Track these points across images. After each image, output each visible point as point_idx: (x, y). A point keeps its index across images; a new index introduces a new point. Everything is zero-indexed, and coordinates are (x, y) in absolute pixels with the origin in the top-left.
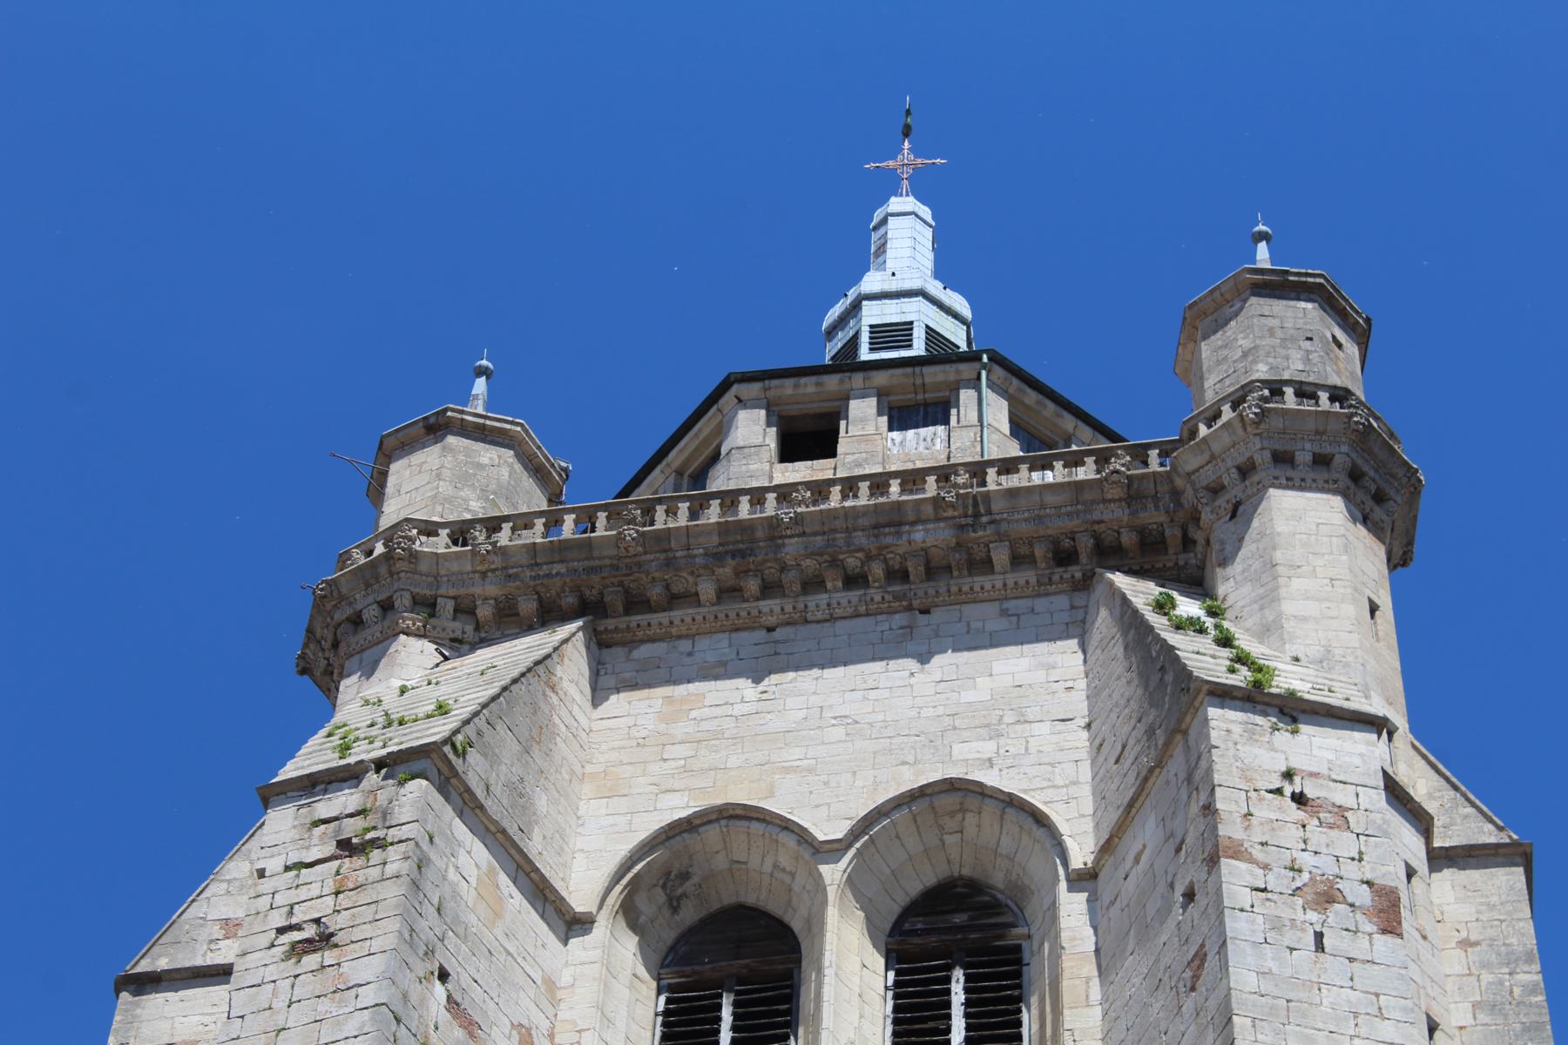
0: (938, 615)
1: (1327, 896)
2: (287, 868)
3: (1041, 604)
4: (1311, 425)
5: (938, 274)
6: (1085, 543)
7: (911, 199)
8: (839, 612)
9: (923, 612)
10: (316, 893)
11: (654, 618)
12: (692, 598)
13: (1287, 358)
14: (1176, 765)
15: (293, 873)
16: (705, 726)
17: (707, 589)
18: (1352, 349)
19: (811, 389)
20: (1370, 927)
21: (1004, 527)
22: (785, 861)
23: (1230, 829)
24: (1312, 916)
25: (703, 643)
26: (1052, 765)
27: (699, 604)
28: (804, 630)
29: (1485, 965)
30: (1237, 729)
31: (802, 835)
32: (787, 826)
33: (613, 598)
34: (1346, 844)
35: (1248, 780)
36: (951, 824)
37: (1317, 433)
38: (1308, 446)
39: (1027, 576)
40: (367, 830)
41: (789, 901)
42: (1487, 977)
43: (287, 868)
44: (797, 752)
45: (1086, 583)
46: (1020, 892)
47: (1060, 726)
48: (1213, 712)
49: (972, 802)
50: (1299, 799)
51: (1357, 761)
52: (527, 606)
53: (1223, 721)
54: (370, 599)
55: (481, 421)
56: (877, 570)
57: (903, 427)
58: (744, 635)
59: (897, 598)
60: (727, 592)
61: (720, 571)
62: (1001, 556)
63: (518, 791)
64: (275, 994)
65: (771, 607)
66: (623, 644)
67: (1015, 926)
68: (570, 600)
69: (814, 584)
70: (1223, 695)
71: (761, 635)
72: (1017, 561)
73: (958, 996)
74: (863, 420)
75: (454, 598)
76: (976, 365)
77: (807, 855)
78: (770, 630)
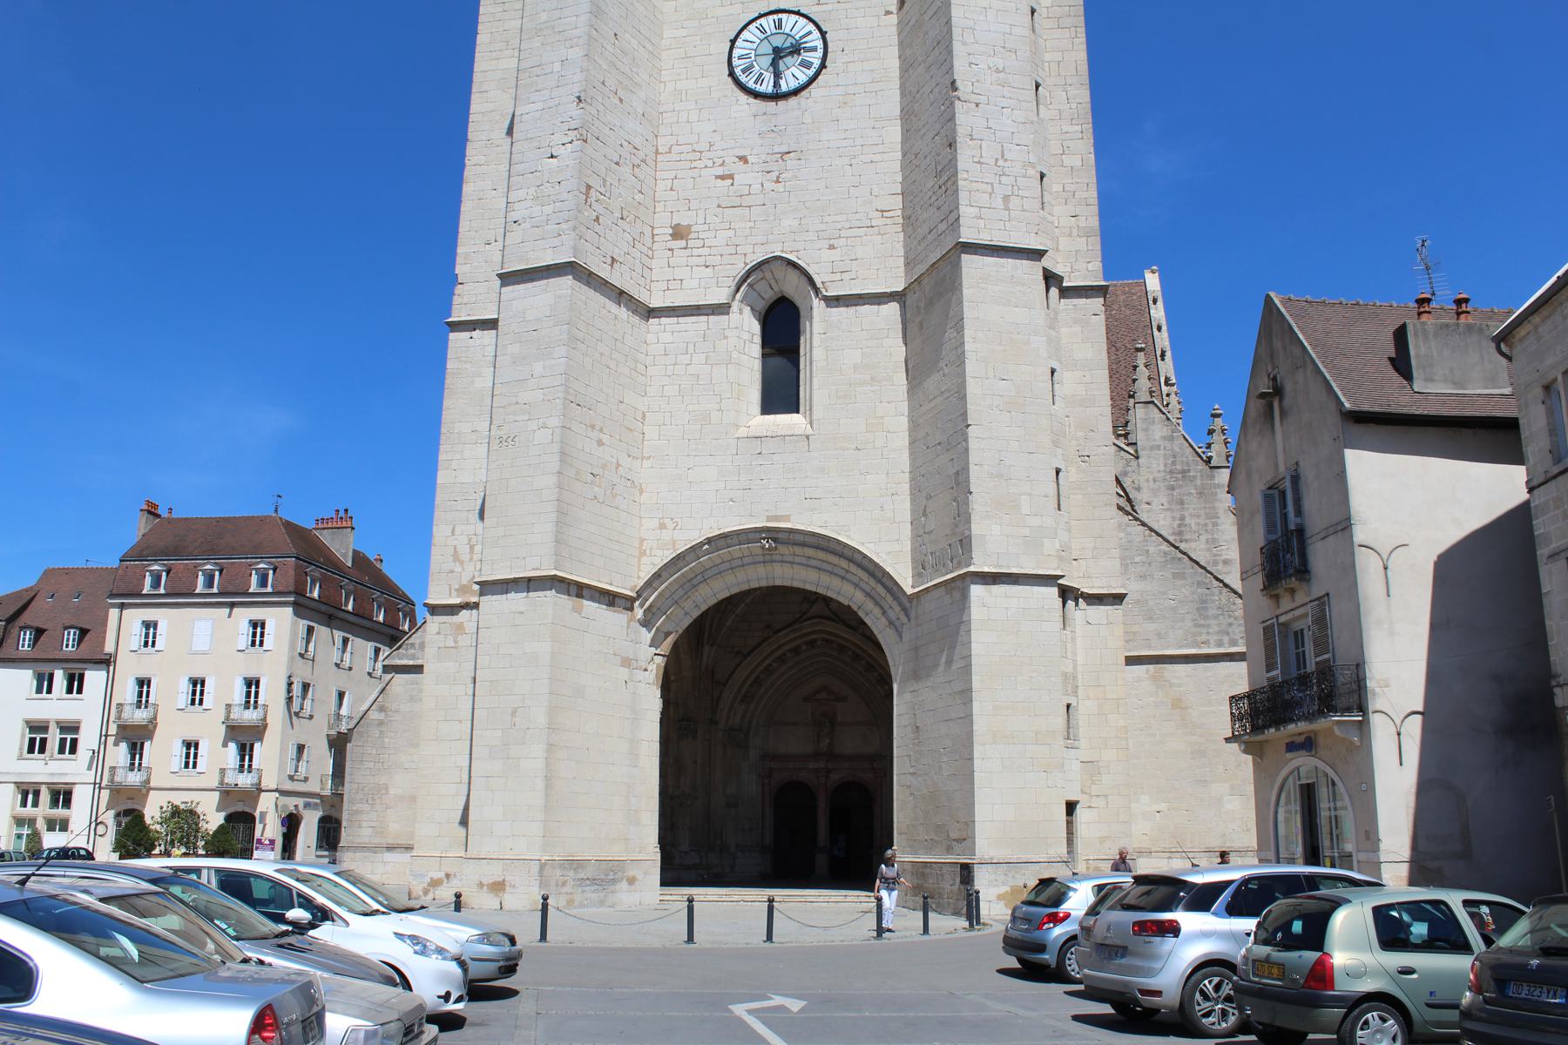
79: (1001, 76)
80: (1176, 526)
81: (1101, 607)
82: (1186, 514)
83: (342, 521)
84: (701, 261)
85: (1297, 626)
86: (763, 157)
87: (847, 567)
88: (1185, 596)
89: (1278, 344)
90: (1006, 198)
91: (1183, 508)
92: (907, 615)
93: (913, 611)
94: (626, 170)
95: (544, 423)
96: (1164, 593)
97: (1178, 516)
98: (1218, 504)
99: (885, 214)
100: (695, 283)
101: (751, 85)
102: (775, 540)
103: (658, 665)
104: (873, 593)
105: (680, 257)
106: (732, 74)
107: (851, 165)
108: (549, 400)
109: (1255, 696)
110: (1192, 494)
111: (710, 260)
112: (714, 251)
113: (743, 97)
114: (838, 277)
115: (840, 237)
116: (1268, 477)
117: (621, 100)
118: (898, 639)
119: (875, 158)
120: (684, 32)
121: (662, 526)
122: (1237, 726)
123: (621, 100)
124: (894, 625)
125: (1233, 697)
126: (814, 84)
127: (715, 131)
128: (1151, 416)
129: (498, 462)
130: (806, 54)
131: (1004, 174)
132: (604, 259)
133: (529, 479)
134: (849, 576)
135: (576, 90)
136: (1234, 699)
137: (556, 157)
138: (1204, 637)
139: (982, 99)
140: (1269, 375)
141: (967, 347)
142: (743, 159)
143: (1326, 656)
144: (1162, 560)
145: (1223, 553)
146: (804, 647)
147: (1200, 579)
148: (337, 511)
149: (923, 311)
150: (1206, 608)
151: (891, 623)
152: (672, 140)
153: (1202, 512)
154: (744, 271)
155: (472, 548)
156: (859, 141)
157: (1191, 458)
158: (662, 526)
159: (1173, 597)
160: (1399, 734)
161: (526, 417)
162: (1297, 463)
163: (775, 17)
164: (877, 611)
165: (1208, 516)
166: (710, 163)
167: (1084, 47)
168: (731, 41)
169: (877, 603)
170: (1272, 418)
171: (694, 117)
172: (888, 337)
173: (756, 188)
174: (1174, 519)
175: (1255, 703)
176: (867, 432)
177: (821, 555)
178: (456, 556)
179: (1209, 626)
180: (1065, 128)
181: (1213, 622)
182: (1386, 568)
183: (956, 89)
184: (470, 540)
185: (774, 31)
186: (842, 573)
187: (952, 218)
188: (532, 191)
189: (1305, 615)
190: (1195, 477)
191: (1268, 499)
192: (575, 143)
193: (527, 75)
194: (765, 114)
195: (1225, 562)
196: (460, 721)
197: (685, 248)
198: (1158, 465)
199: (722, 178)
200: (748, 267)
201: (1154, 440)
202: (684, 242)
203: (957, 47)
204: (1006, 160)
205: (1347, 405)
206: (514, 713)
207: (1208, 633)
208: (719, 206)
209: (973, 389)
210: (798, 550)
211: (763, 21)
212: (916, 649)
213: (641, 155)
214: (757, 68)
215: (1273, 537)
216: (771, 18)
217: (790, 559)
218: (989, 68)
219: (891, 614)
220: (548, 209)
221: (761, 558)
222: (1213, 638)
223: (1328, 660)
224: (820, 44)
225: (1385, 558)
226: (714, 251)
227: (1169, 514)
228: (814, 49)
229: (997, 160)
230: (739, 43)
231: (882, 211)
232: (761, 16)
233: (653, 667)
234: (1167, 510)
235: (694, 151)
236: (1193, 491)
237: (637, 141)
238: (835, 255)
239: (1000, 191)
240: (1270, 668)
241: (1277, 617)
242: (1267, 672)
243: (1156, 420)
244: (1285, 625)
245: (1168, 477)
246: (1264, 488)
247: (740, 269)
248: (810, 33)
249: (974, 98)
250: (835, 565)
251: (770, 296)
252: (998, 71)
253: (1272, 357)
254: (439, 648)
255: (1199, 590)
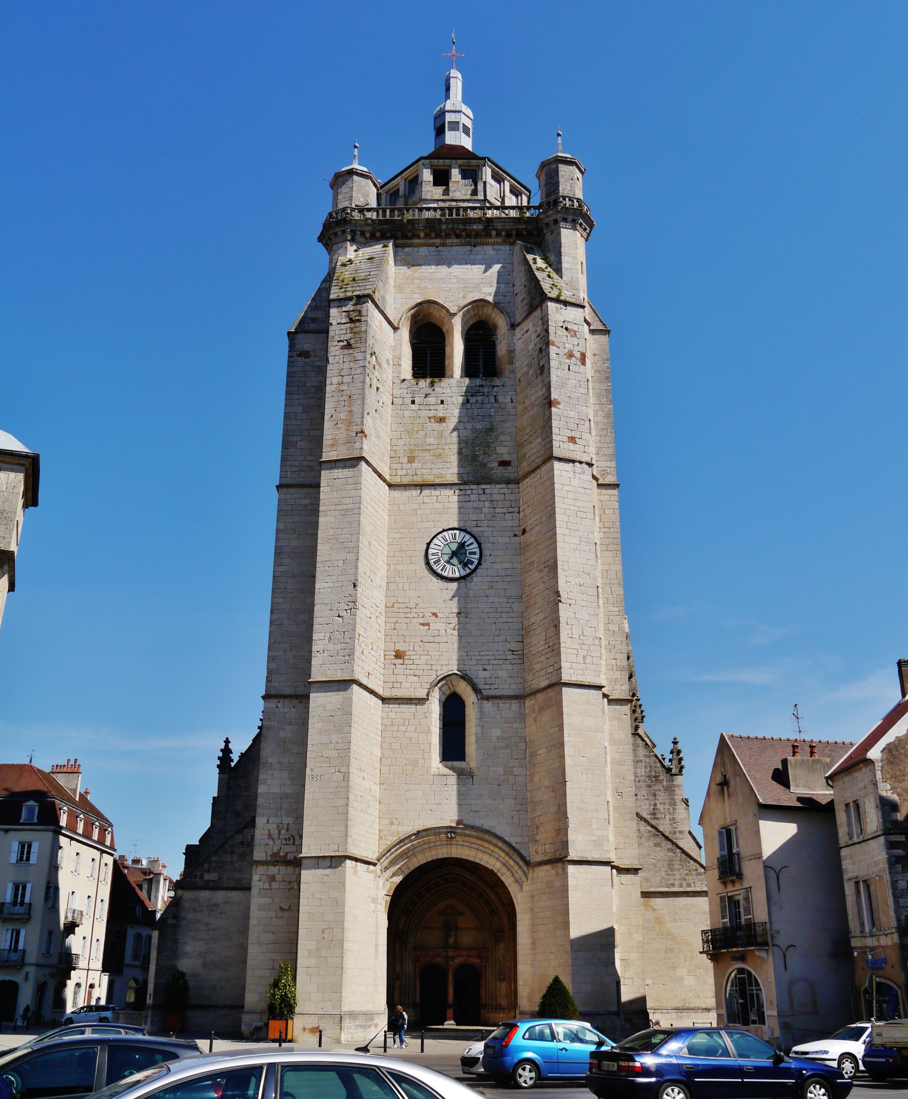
0: (478, 248)
1: (570, 355)
2: (338, 324)
3: (502, 247)
4: (573, 211)
5: (465, 101)
6: (514, 232)
7: (456, 71)
8: (454, 244)
9: (475, 246)
10: (345, 332)
11: (409, 241)
12: (419, 237)
13: (566, 185)
14: (538, 313)
15: (338, 326)
16: (423, 275)
17: (422, 234)
18: (581, 179)
19: (442, 164)
20: (579, 364)
21: (495, 227)
22: (442, 315)
23: (552, 338)
24: (568, 361)
25: (421, 249)
26: (505, 296)
27: (419, 238)
28: (445, 249)
29: (598, 361)
30: (554, 309)
31: (447, 310)
32: (444, 307)
33: (399, 234)
34: (576, 341)
35: (555, 323)
36: (480, 309)
37: (573, 213)
38: (571, 217)
39: (499, 240)
40: (356, 316)
41: (442, 325)
42: (599, 364)
43: (338, 324)
44: (445, 285)
45: (513, 244)
46: (495, 327)
47: (507, 285)
48: (549, 304)
49: (487, 304)
50: (566, 329)
51: (579, 318)
52: (378, 234)
53: (551, 305)
54: (339, 229)
55: (361, 172)
56: (464, 234)
57: (465, 179)
58: (431, 249)
59: (468, 242)
60: (427, 236)
61: (426, 231)
62: (494, 233)
63: (383, 297)
64: (339, 359)
65: (437, 241)
66: (401, 247)
67: (493, 335)
68: (389, 234)
69: (448, 236)
70: (552, 300)
71: (434, 248)
72: (498, 235)
73: (481, 353)
74: (455, 175)
75: (360, 231)
76: (484, 161)
77: (448, 316)
78: (437, 247)
79: (582, 588)
80: (651, 810)
81: (629, 876)
82: (658, 802)
83: (73, 770)
84: (412, 672)
85: (737, 898)
86: (447, 615)
87: (493, 849)
88: (661, 857)
89: (727, 761)
90: (584, 657)
91: (656, 799)
92: (526, 877)
93: (530, 875)
94: (373, 619)
95: (339, 769)
96: (649, 855)
97: (653, 803)
98: (676, 797)
99: (514, 653)
100: (409, 685)
101: (439, 571)
102: (454, 833)
103: (386, 901)
104: (507, 864)
105: (400, 669)
106: (428, 563)
107: (495, 623)
108: (341, 757)
109: (715, 932)
110: (660, 790)
111: (417, 673)
112: (419, 667)
113: (434, 579)
114: (488, 687)
115: (489, 664)
116: (721, 823)
117: (371, 580)
118: (520, 890)
119: (510, 620)
120: (400, 535)
121: (392, 823)
122: (705, 946)
123: (371, 580)
124: (518, 882)
125: (703, 931)
126: (474, 574)
127: (419, 597)
128: (638, 742)
129: (312, 789)
130: (470, 556)
131: (583, 644)
132: (365, 674)
133: (330, 800)
134: (494, 854)
135: (352, 578)
136: (704, 932)
137: (342, 617)
138: (672, 882)
139: (573, 602)
140: (722, 773)
141: (565, 739)
142: (435, 615)
143: (750, 917)
144: (648, 835)
145: (679, 826)
146: (442, 882)
147: (669, 847)
148: (69, 760)
149: (536, 712)
150: (673, 865)
151: (516, 881)
152: (394, 600)
153: (667, 801)
154: (436, 681)
155: (279, 832)
156: (499, 610)
157: (660, 769)
158: (392, 823)
159: (653, 857)
160: (784, 956)
161: (328, 765)
162: (736, 821)
163: (452, 532)
164: (508, 874)
165: (670, 804)
166: (416, 616)
167: (620, 562)
168: (427, 543)
169: (509, 869)
170: (724, 795)
171: (407, 587)
172: (515, 722)
173: (442, 632)
174: (650, 805)
175: (716, 935)
176: (504, 775)
177: (479, 842)
178: (270, 836)
179: (675, 875)
180: (611, 609)
181: (676, 873)
182: (778, 877)
183: (559, 596)
184: (278, 826)
185: (452, 541)
186: (490, 852)
187: (556, 666)
188: (328, 635)
189: (740, 894)
190: (663, 780)
191: (720, 833)
192: (353, 610)
193: (322, 565)
194: (447, 589)
195: (680, 832)
196: (273, 933)
197: (403, 664)
198: (641, 772)
199: (423, 625)
200: (439, 678)
201: (639, 757)
202: (402, 660)
203: (560, 571)
204: (584, 636)
205: (761, 801)
206: (323, 932)
207: (674, 879)
208: (422, 641)
209: (568, 762)
210: (466, 839)
211: (445, 533)
212: (532, 896)
213: (379, 610)
214: (442, 562)
215: (722, 853)
216: (450, 532)
217: (462, 843)
218: (576, 584)
219: (516, 875)
220: (339, 647)
221: (445, 843)
222: (677, 883)
223: (750, 919)
224: (477, 550)
225: (777, 872)
226: (419, 667)
227: (647, 802)
228: (474, 553)
229: (580, 636)
230: (432, 545)
231: (512, 651)
232: (444, 531)
233: (384, 903)
234: (646, 799)
235: (407, 607)
236: (662, 789)
237: (378, 603)
238: (486, 674)
239: (582, 653)
240: (723, 917)
241: (727, 893)
242: (722, 919)
243: (640, 745)
244: (730, 898)
245: (647, 780)
246: (718, 828)
247: (433, 678)
248: (472, 544)
249: (569, 601)
250: (486, 848)
251: (448, 692)
252: (580, 585)
253: (724, 765)
254: (260, 889)
255: (669, 854)
